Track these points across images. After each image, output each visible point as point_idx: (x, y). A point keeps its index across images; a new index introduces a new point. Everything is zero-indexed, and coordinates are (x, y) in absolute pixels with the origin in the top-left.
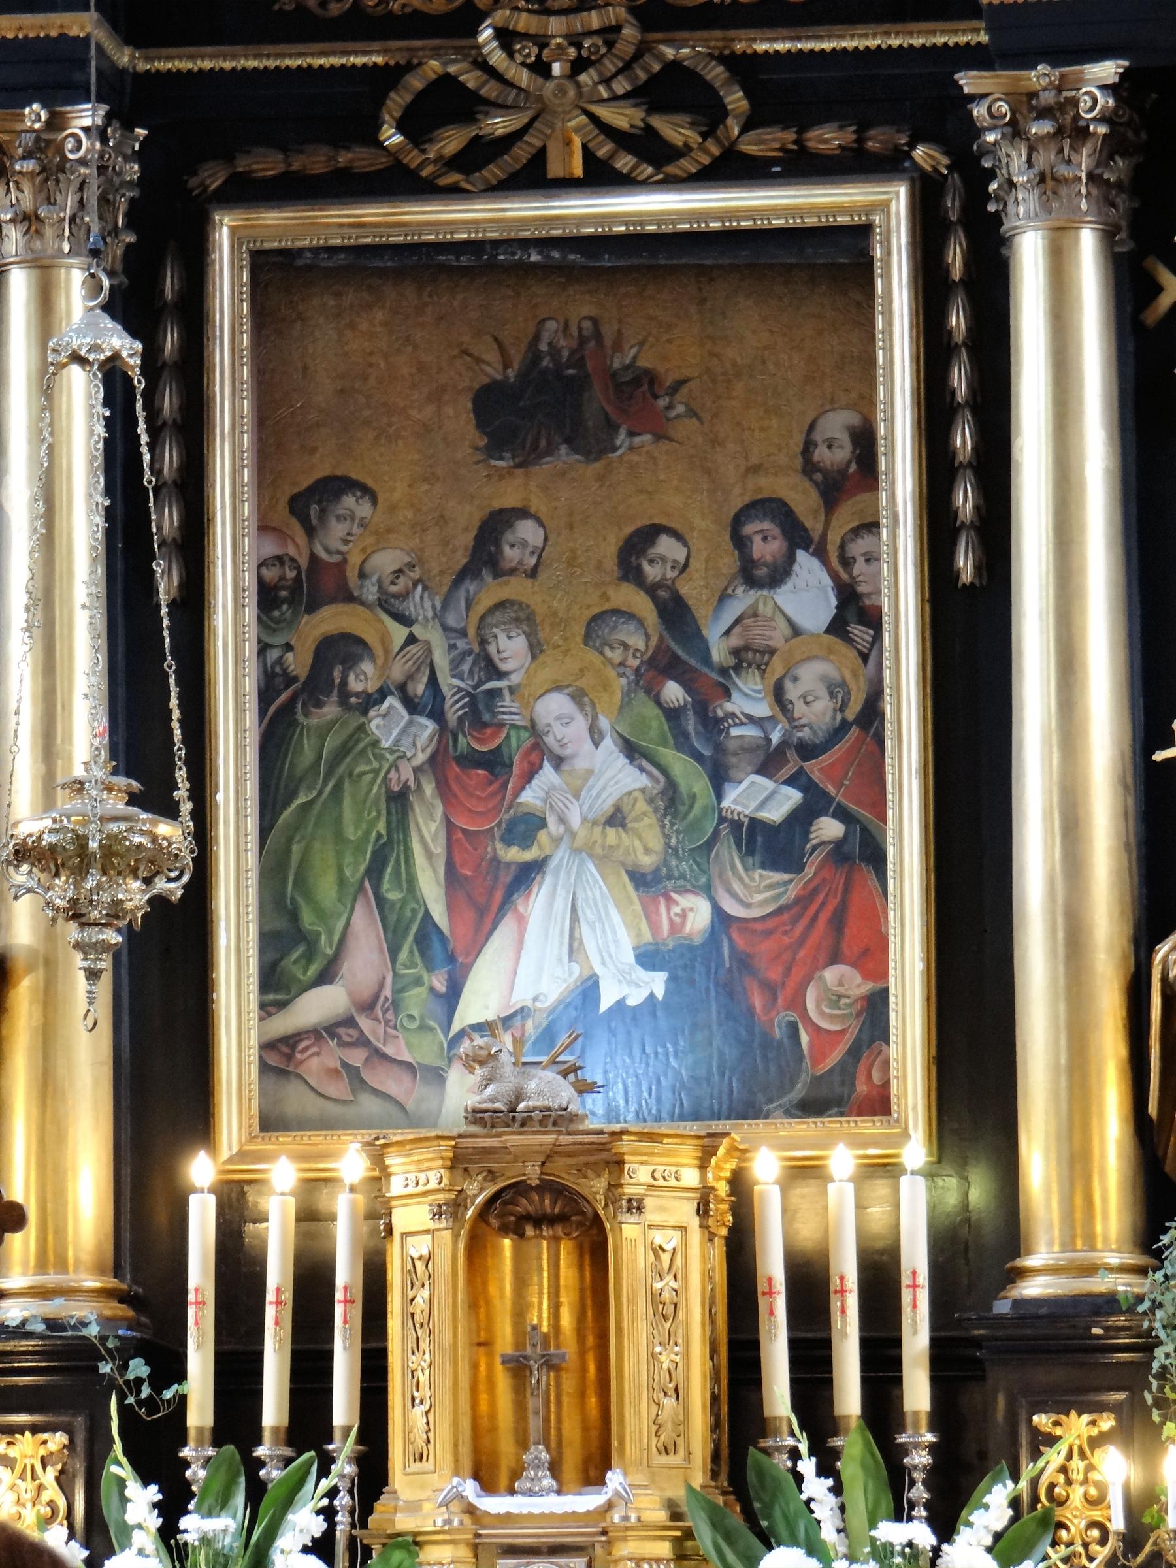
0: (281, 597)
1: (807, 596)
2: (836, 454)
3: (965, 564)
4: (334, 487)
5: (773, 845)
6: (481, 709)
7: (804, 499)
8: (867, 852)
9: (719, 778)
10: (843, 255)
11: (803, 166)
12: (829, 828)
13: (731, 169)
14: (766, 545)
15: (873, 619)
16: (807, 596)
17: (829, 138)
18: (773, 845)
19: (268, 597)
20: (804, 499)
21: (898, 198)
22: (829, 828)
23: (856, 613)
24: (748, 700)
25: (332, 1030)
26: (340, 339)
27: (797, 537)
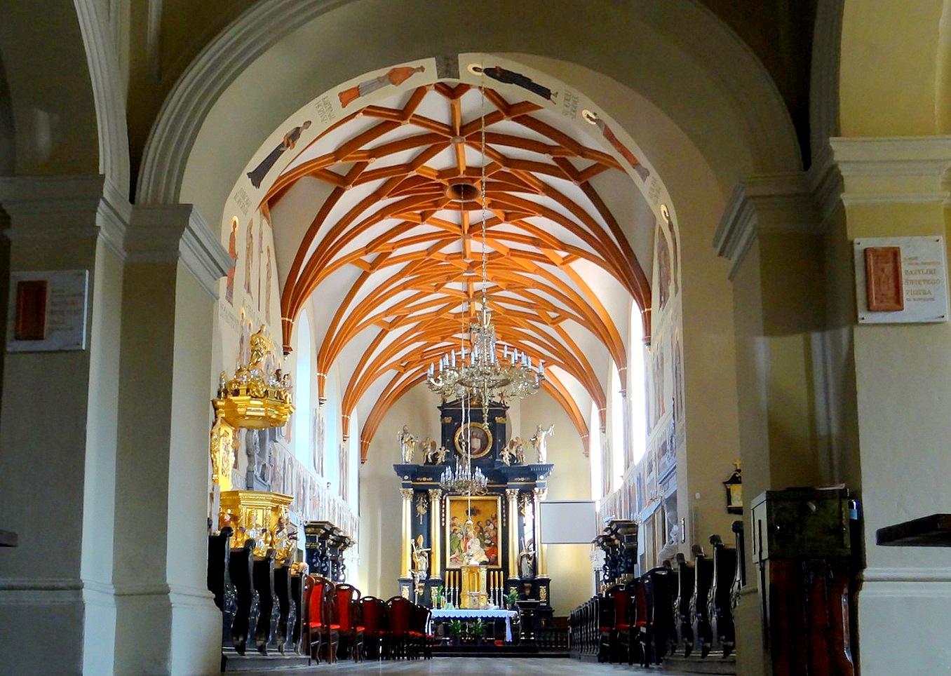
0: (452, 525)
1: (491, 527)
2: (494, 516)
3: (504, 525)
4: (455, 517)
5: (489, 545)
6: (466, 534)
7: (491, 520)
8: (496, 546)
9: (484, 540)
10: (496, 501)
11: (492, 495)
12: (493, 544)
13: (487, 495)
14: (488, 523)
15: (497, 529)
16: (491, 527)
17: (494, 493)
18: (489, 545)
19: (450, 526)
20: (491, 520)
21: (500, 498)
22: (493, 544)
23: (496, 528)
24: (487, 534)
25: (455, 558)
26: (456, 506)
27: (491, 522)
